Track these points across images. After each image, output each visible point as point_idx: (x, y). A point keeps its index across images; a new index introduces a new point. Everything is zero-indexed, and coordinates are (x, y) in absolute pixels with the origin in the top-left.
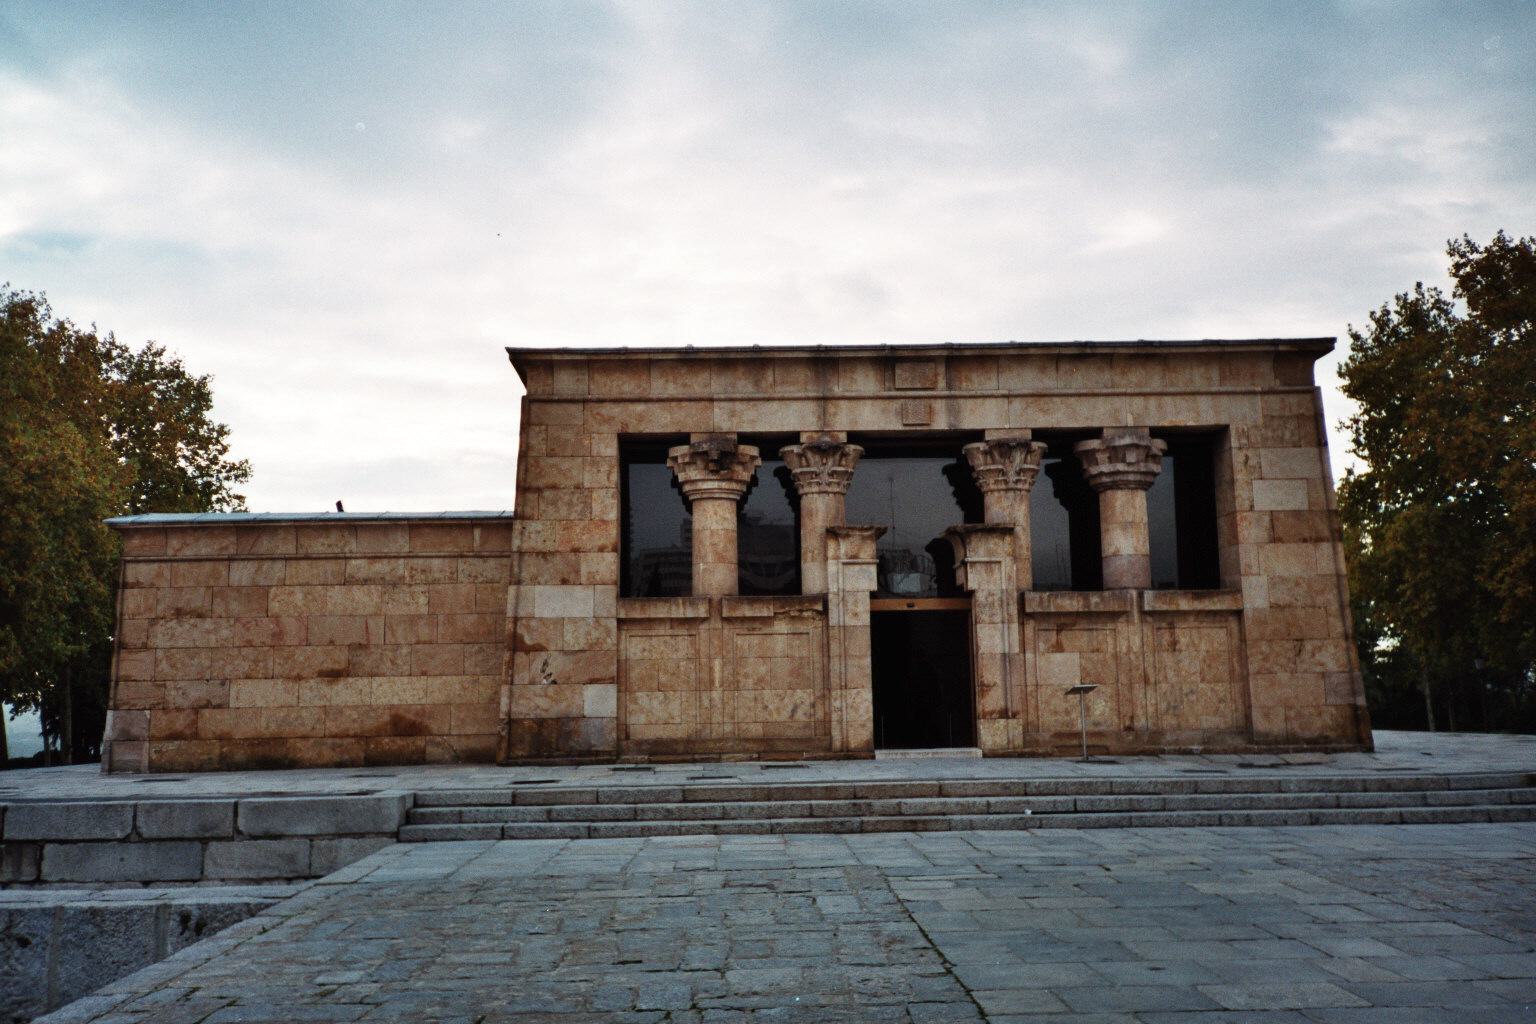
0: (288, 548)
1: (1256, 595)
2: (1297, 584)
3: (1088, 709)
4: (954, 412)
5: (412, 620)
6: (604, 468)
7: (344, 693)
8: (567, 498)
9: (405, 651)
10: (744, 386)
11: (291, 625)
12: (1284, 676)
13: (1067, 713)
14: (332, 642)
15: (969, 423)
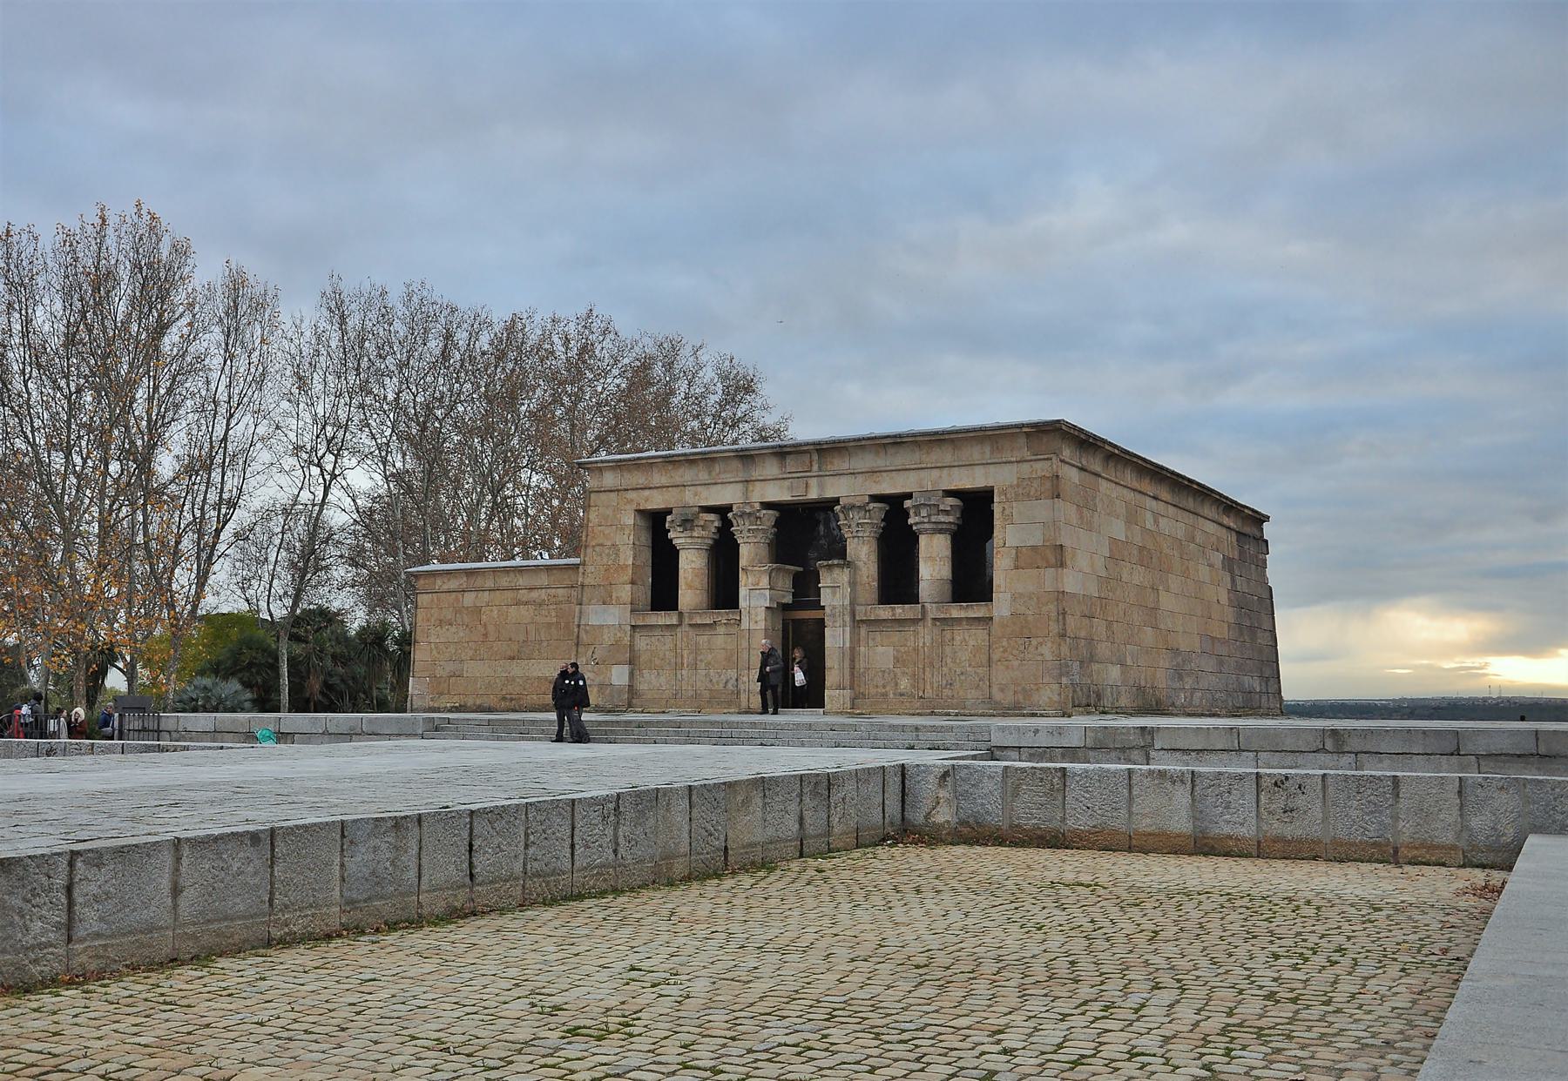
0: (489, 584)
1: (1001, 605)
2: (1030, 598)
3: (896, 684)
4: (821, 487)
5: (549, 625)
6: (627, 532)
7: (517, 669)
8: (607, 551)
9: (545, 644)
10: (703, 476)
11: (491, 628)
12: (1016, 663)
13: (884, 687)
14: (510, 640)
15: (830, 494)
